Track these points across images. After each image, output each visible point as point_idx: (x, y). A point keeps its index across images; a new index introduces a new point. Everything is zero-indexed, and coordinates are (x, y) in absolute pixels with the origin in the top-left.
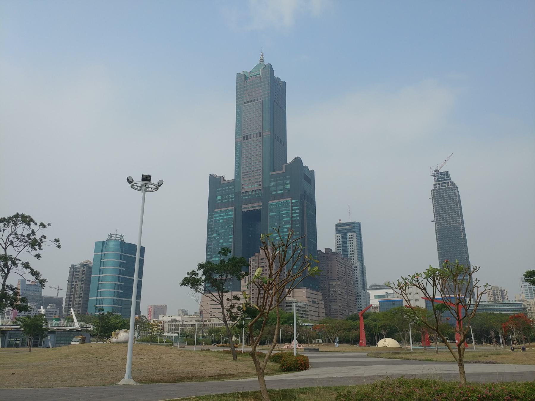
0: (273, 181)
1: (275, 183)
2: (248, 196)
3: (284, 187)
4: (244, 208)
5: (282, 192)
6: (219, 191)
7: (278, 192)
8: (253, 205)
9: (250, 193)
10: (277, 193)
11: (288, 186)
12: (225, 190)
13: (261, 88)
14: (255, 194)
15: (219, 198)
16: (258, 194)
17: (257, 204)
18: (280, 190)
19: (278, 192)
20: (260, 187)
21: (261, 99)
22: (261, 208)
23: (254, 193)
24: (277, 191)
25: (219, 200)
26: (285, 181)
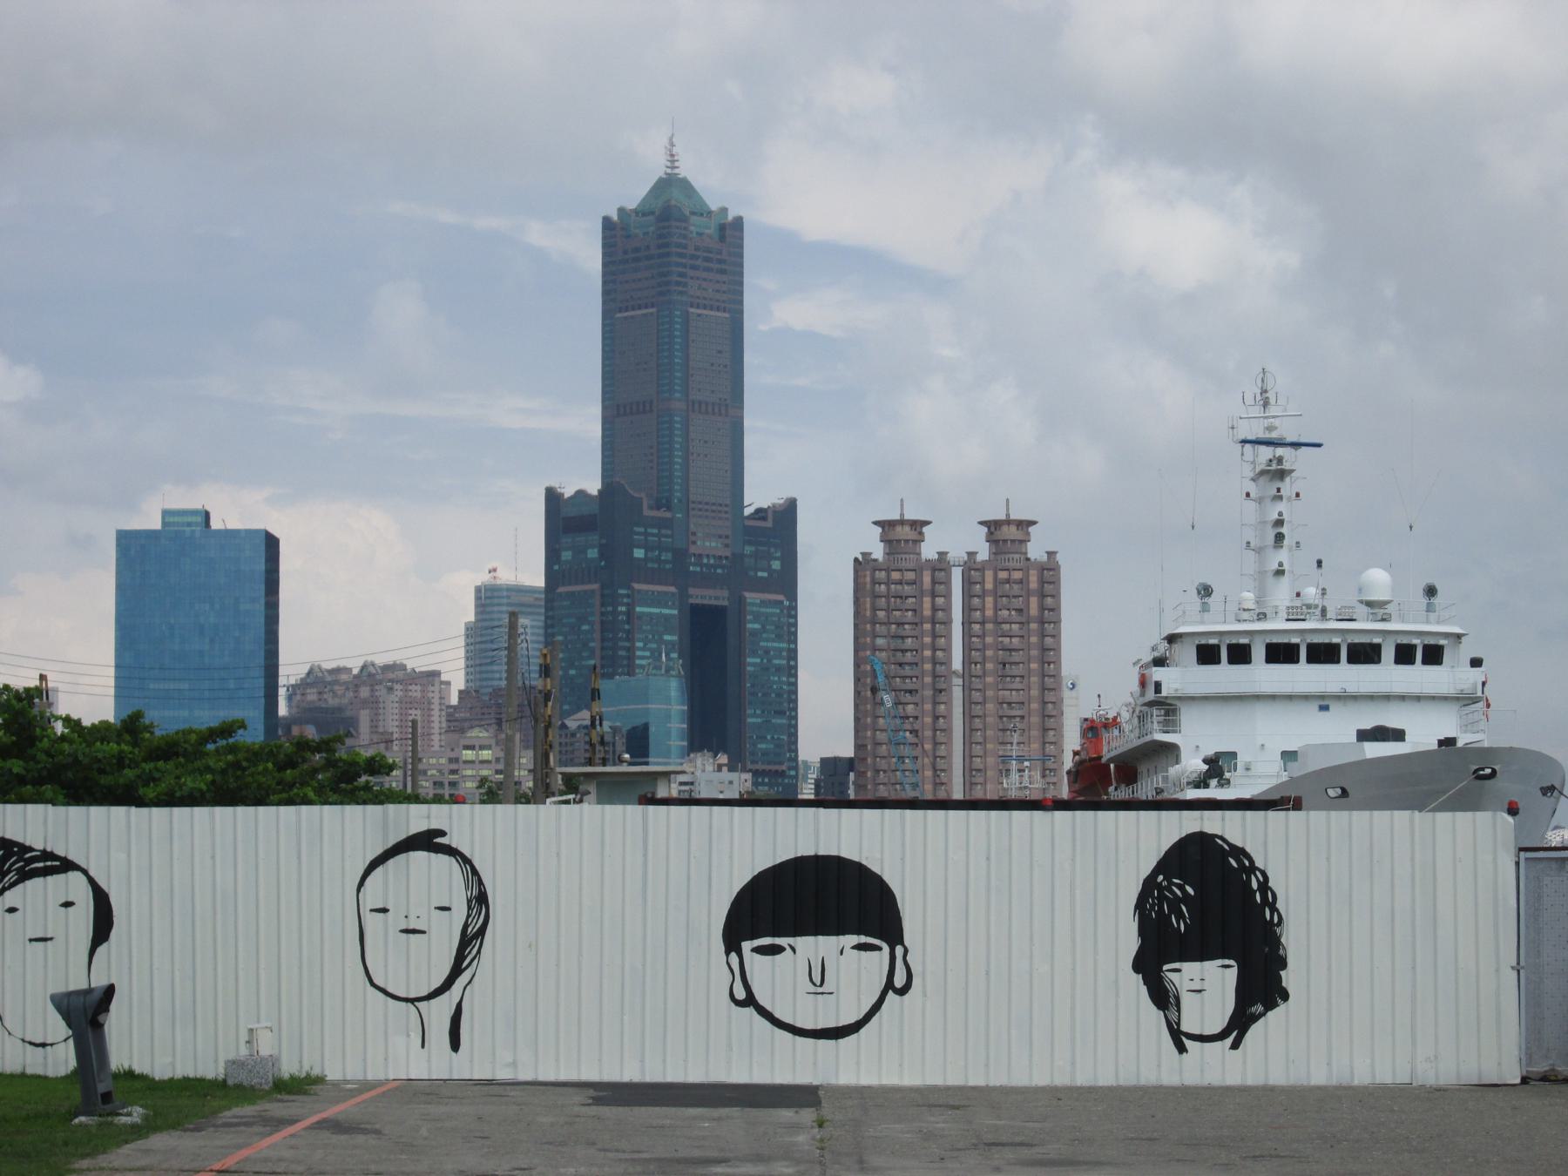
0: (750, 543)
1: (753, 549)
2: (702, 565)
3: (770, 566)
4: (691, 596)
5: (765, 574)
6: (638, 534)
7: (760, 574)
8: (710, 592)
9: (705, 561)
10: (756, 574)
11: (776, 565)
12: (653, 535)
13: (724, 278)
14: (715, 567)
15: (639, 553)
16: (722, 567)
17: (718, 593)
18: (763, 570)
19: (760, 574)
20: (728, 553)
21: (725, 311)
22: (726, 603)
23: (712, 561)
24: (757, 570)
25: (639, 559)
26: (772, 550)
